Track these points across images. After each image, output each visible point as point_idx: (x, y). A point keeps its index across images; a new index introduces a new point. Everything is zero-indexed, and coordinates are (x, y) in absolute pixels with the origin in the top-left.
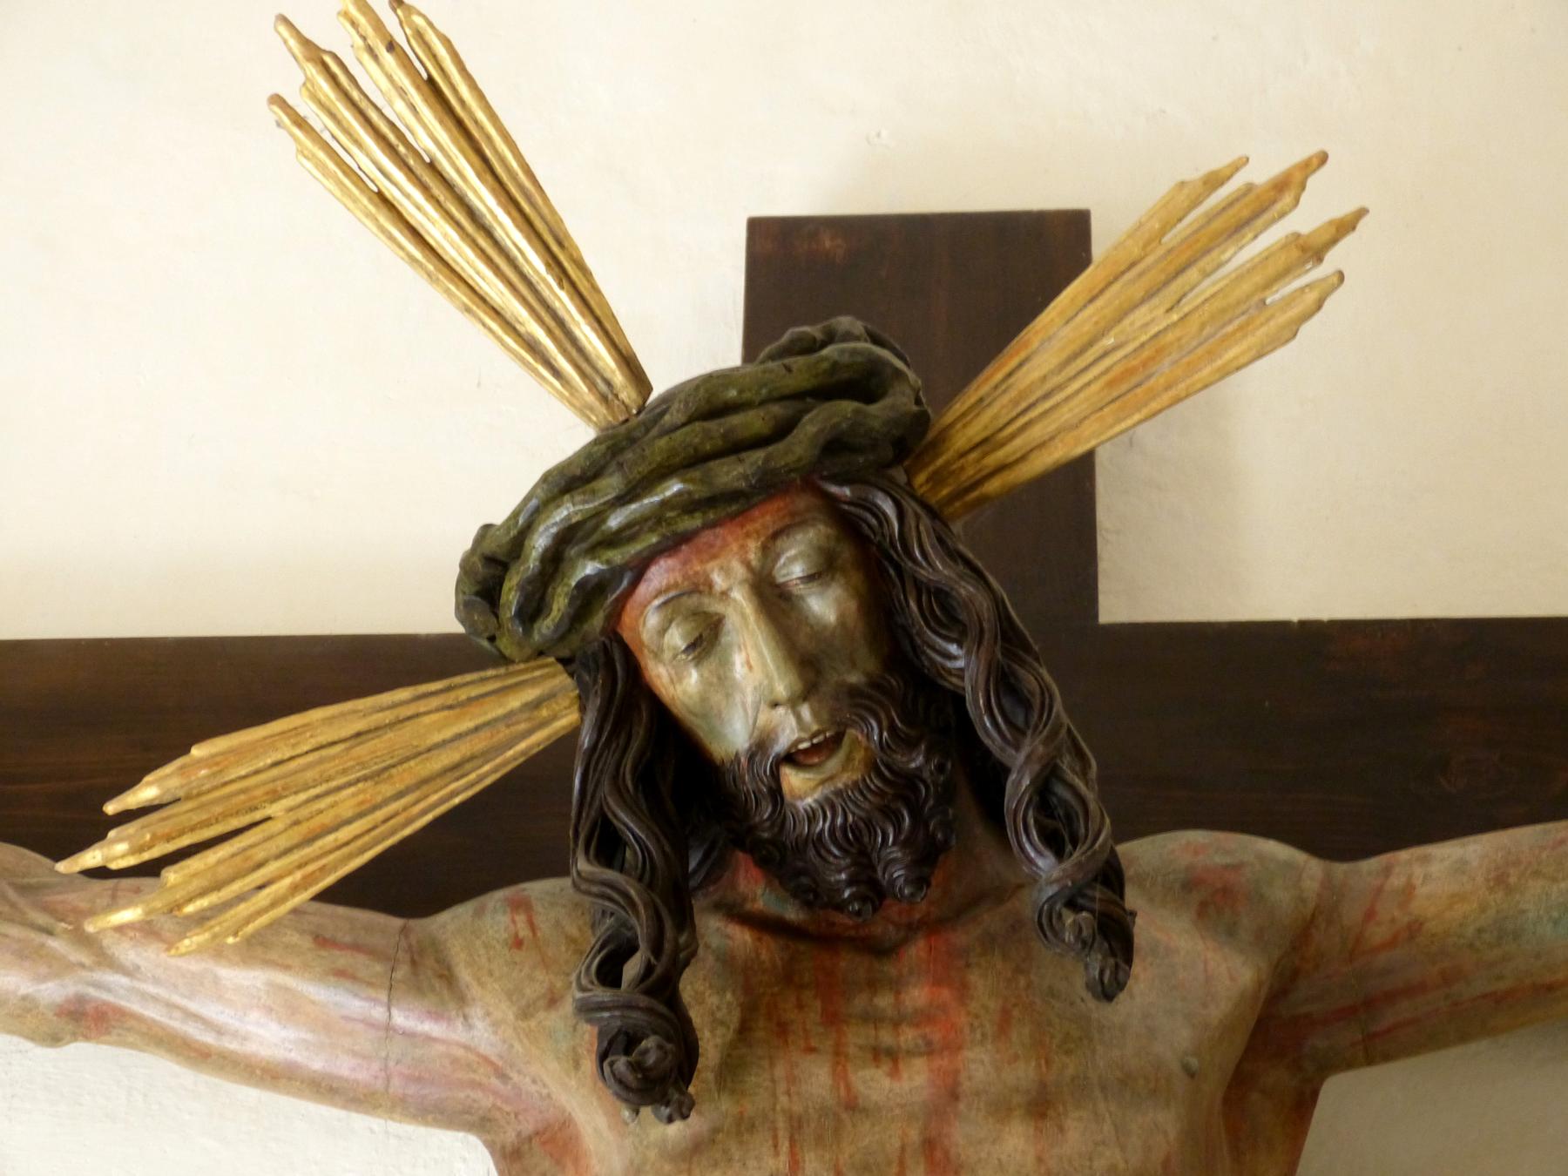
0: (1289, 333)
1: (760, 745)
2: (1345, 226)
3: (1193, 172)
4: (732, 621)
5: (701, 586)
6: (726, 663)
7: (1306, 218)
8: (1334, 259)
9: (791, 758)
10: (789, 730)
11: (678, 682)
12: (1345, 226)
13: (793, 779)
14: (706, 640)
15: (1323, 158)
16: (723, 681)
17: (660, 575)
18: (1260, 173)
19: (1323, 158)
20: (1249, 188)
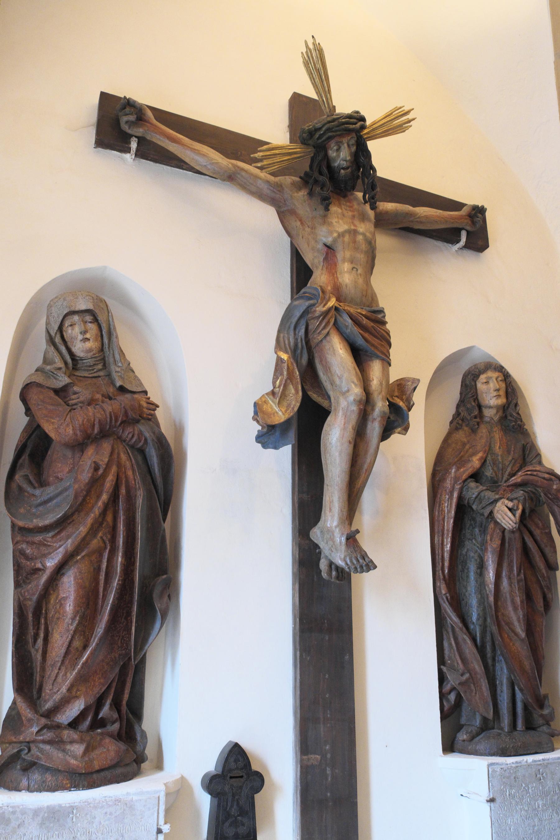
0: (404, 131)
1: (339, 165)
2: (414, 119)
3: (399, 106)
4: (342, 147)
5: (341, 142)
6: (340, 153)
7: (410, 116)
8: (412, 123)
9: (343, 169)
10: (344, 164)
11: (332, 153)
12: (414, 119)
13: (342, 171)
14: (338, 150)
15: (413, 109)
16: (338, 156)
17: (337, 139)
18: (406, 109)
19: (413, 109)
20: (404, 110)
